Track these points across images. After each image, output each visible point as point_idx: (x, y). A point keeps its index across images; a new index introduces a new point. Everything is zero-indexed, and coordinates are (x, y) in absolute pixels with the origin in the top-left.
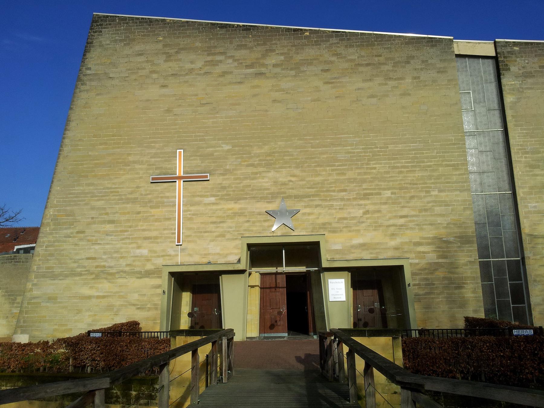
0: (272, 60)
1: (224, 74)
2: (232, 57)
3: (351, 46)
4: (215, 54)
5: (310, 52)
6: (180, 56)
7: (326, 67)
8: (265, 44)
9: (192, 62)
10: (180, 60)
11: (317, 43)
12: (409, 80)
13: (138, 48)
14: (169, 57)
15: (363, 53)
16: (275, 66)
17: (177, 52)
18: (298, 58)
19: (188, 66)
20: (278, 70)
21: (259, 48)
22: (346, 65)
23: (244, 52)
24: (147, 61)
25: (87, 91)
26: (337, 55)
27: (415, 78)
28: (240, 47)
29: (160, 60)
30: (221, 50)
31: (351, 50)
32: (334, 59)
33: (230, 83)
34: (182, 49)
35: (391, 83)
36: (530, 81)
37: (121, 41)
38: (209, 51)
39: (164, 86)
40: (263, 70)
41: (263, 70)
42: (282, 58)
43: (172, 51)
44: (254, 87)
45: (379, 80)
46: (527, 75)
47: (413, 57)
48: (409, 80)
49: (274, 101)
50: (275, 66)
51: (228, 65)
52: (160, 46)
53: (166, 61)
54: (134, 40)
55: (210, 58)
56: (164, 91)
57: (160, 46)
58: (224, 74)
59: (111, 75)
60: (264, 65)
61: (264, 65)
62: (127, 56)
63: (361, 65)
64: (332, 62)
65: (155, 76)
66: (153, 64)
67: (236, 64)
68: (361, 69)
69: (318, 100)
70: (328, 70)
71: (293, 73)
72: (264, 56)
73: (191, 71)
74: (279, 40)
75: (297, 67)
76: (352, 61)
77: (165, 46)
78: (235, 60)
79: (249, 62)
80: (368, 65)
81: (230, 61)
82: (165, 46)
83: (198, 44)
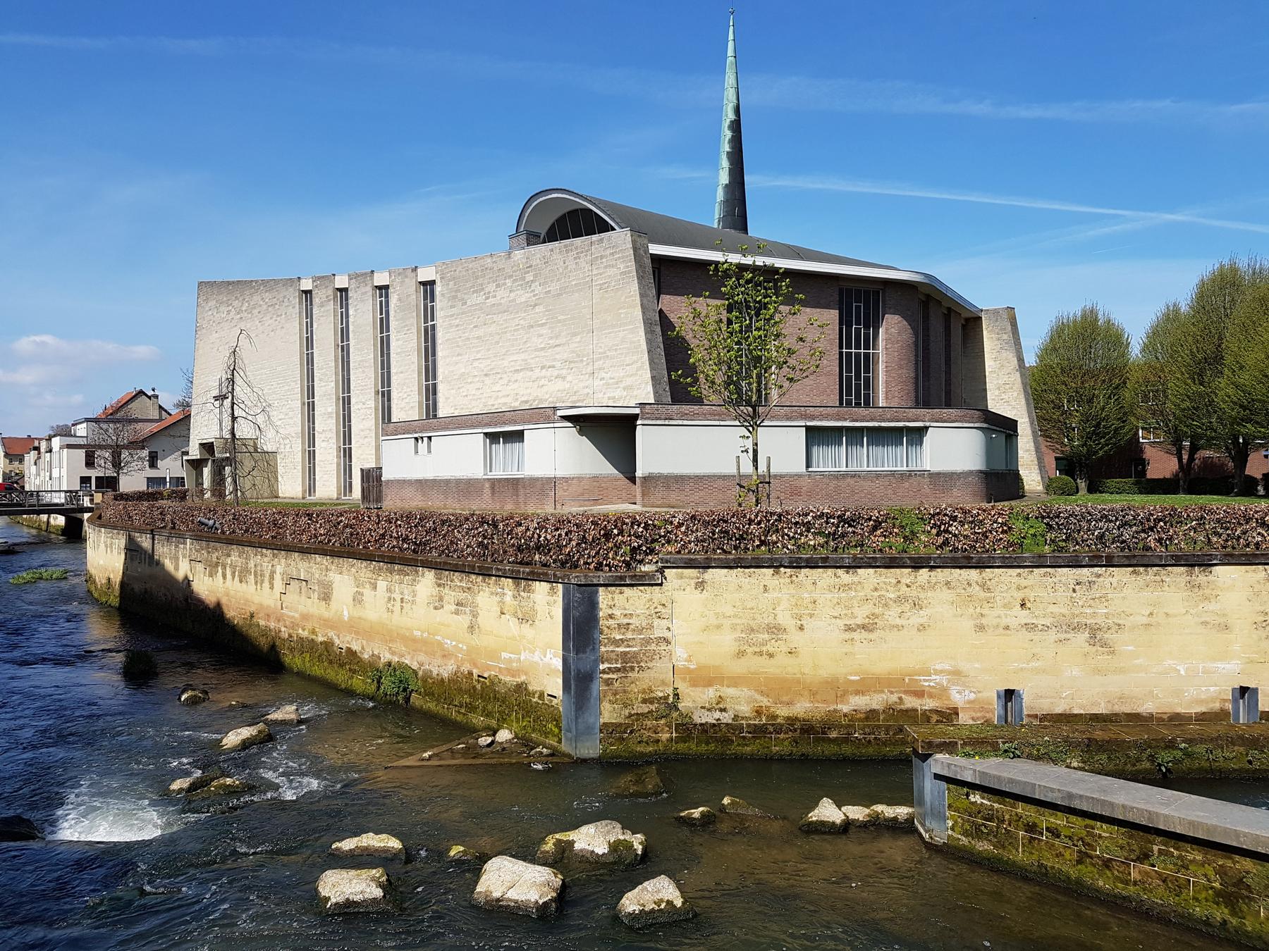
31: (267, 294)
68: (270, 309)
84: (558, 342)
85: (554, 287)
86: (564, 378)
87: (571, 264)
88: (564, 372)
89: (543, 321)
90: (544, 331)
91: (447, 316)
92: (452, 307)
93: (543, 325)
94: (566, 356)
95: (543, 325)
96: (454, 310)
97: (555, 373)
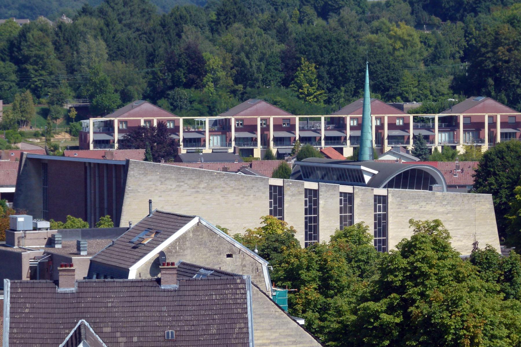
0: (202, 185)
1: (184, 191)
2: (186, 183)
3: (232, 180)
4: (180, 182)
5: (217, 182)
6: (166, 183)
7: (222, 189)
8: (199, 178)
9: (171, 186)
10: (166, 184)
11: (219, 178)
12: (252, 196)
13: (149, 177)
14: (162, 183)
15: (236, 184)
16: (203, 188)
17: (165, 181)
18: (213, 185)
19: (169, 187)
20: (204, 190)
21: (197, 180)
22: (230, 189)
23: (191, 181)
24: (154, 184)
25: (129, 198)
26: (226, 184)
27: (254, 195)
28: (191, 179)
29: (159, 184)
30: (183, 180)
31: (232, 182)
32: (225, 186)
33: (186, 196)
34: (168, 179)
35: (246, 197)
36: (294, 198)
37: (143, 174)
38: (178, 180)
39: (160, 196)
40: (199, 190)
41: (199, 190)
42: (206, 184)
43: (163, 180)
44: (195, 198)
45: (241, 196)
46: (294, 195)
47: (253, 186)
48: (252, 196)
49: (203, 204)
50: (203, 188)
51: (185, 187)
52: (158, 177)
53: (161, 184)
54: (147, 174)
55: (178, 184)
56: (161, 199)
57: (158, 177)
58: (184, 191)
59: (139, 191)
60: (199, 188)
61: (199, 188)
62: (145, 181)
63: (235, 189)
64: (224, 187)
65: (156, 191)
66: (156, 186)
67: (188, 187)
68: (235, 191)
69: (219, 204)
70: (223, 191)
71: (210, 191)
72: (199, 183)
73: (171, 189)
74: (205, 176)
75: (211, 189)
76: (231, 187)
77: (160, 177)
78: (188, 185)
79: (193, 186)
80: (238, 189)
81: (186, 185)
82: (160, 177)
83: (173, 177)
84: (459, 228)
85: (457, 208)
86: (461, 241)
87: (466, 201)
88: (462, 239)
89: (452, 219)
90: (452, 223)
91: (395, 212)
92: (398, 208)
93: (451, 221)
94: (462, 233)
95: (451, 221)
96: (399, 210)
97: (457, 239)
